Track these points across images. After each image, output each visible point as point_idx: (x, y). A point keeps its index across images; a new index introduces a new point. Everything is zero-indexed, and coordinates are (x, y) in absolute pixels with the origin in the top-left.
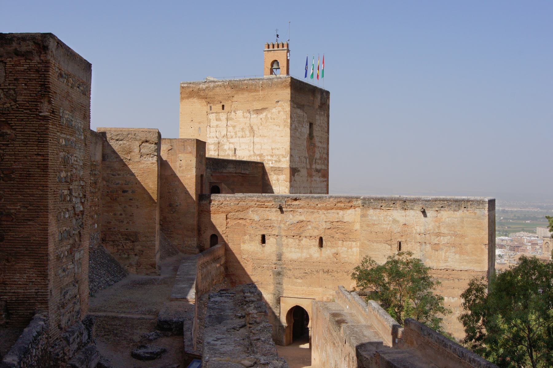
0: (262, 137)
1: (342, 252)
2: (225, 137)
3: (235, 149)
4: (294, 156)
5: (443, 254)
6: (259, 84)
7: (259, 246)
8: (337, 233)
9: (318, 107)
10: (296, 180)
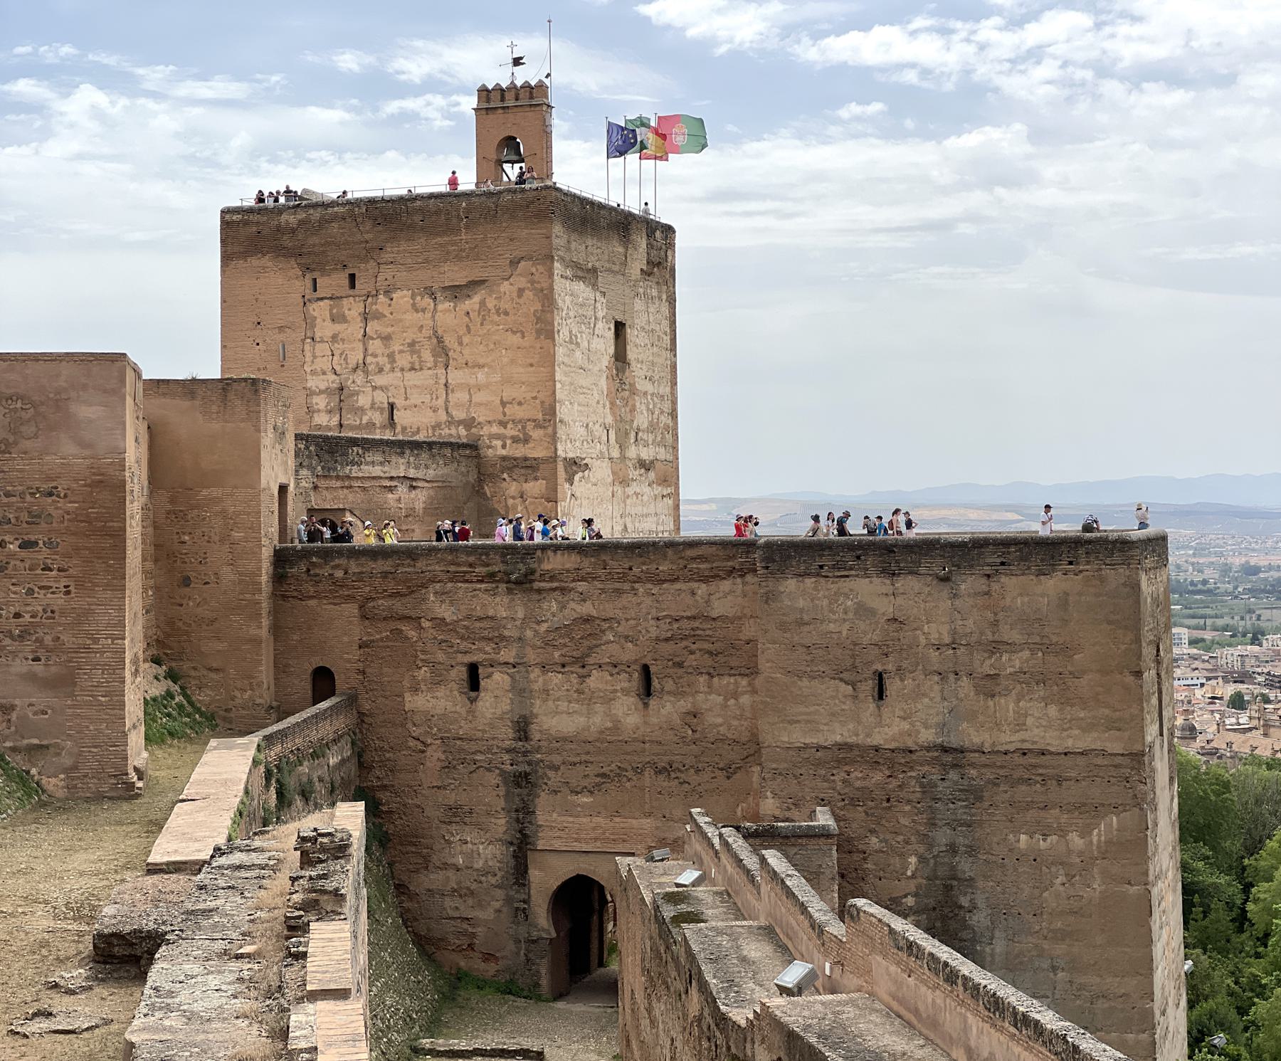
0: (473, 367)
1: (710, 710)
2: (359, 372)
3: (392, 407)
4: (571, 423)
5: (1011, 706)
6: (457, 210)
7: (459, 699)
8: (692, 653)
9: (639, 272)
10: (578, 494)
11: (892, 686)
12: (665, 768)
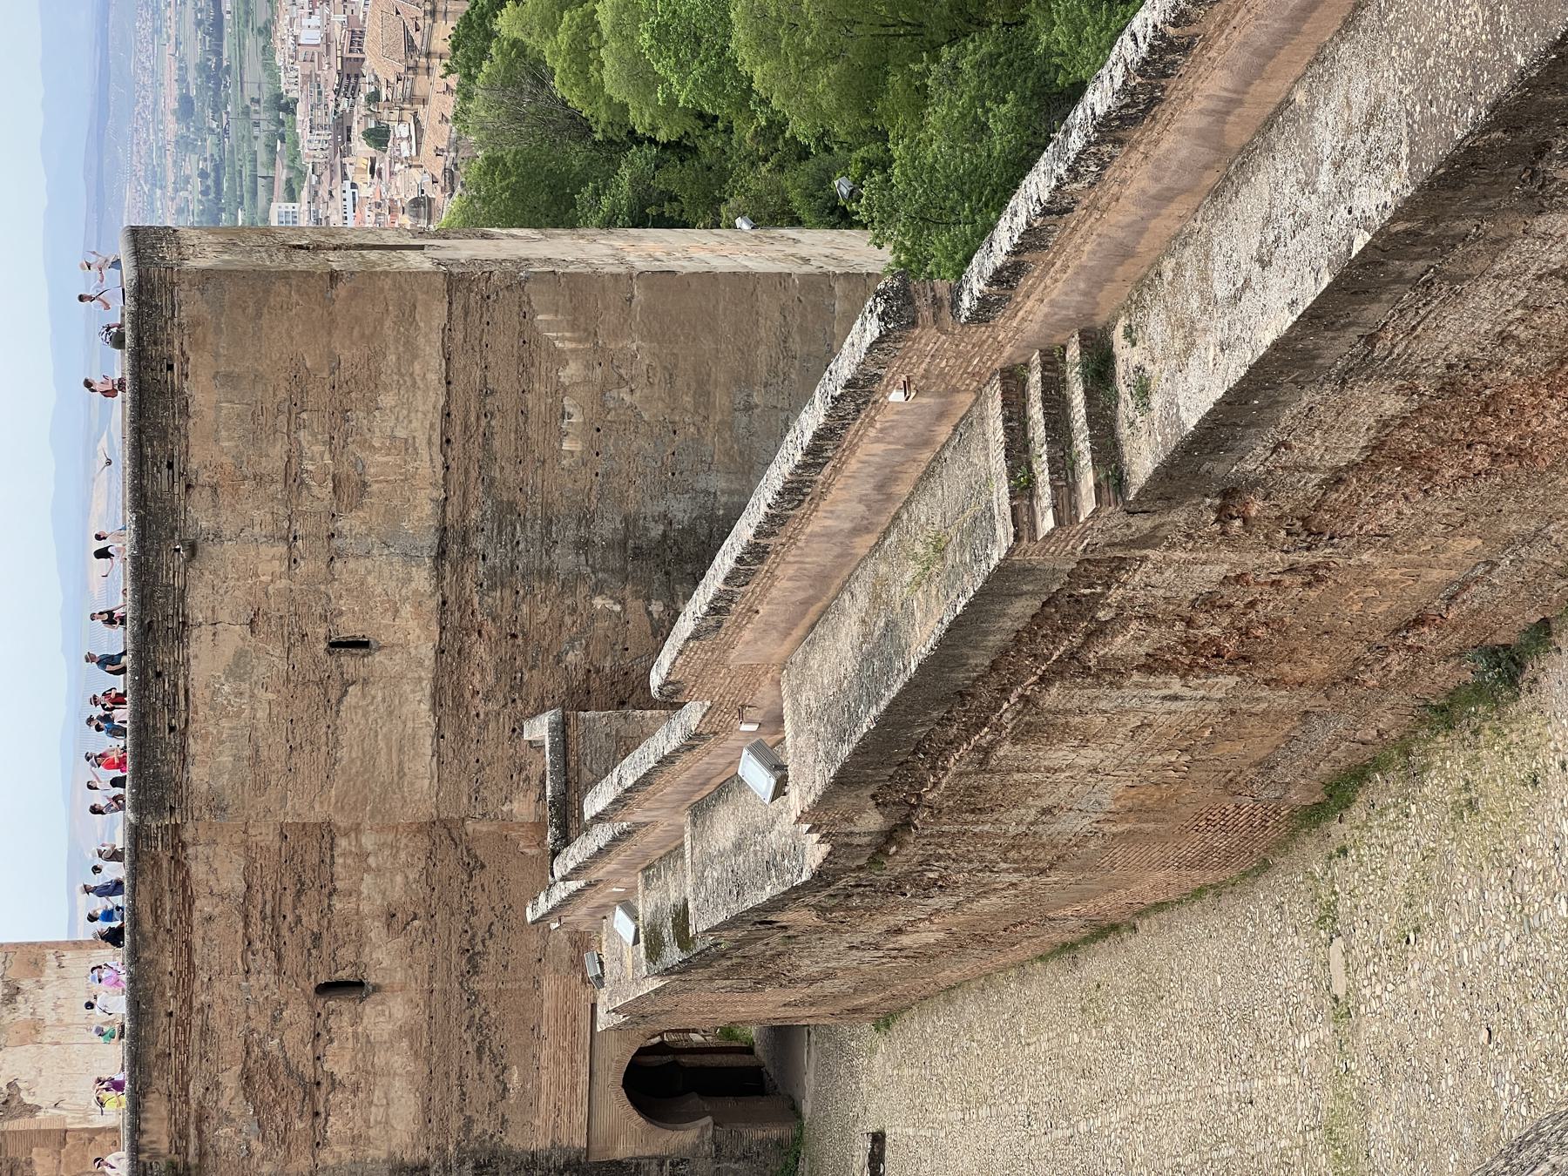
5: (379, 458)
8: (299, 920)
10: (54, 1099)
11: (349, 627)
12: (469, 960)
